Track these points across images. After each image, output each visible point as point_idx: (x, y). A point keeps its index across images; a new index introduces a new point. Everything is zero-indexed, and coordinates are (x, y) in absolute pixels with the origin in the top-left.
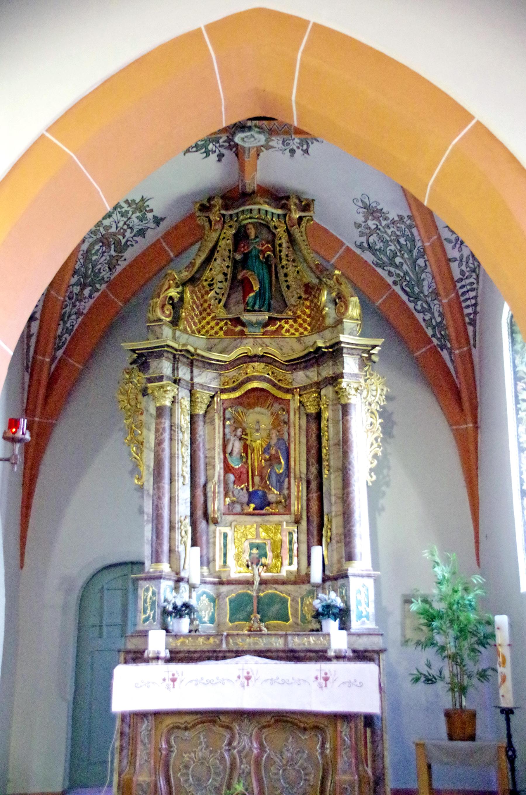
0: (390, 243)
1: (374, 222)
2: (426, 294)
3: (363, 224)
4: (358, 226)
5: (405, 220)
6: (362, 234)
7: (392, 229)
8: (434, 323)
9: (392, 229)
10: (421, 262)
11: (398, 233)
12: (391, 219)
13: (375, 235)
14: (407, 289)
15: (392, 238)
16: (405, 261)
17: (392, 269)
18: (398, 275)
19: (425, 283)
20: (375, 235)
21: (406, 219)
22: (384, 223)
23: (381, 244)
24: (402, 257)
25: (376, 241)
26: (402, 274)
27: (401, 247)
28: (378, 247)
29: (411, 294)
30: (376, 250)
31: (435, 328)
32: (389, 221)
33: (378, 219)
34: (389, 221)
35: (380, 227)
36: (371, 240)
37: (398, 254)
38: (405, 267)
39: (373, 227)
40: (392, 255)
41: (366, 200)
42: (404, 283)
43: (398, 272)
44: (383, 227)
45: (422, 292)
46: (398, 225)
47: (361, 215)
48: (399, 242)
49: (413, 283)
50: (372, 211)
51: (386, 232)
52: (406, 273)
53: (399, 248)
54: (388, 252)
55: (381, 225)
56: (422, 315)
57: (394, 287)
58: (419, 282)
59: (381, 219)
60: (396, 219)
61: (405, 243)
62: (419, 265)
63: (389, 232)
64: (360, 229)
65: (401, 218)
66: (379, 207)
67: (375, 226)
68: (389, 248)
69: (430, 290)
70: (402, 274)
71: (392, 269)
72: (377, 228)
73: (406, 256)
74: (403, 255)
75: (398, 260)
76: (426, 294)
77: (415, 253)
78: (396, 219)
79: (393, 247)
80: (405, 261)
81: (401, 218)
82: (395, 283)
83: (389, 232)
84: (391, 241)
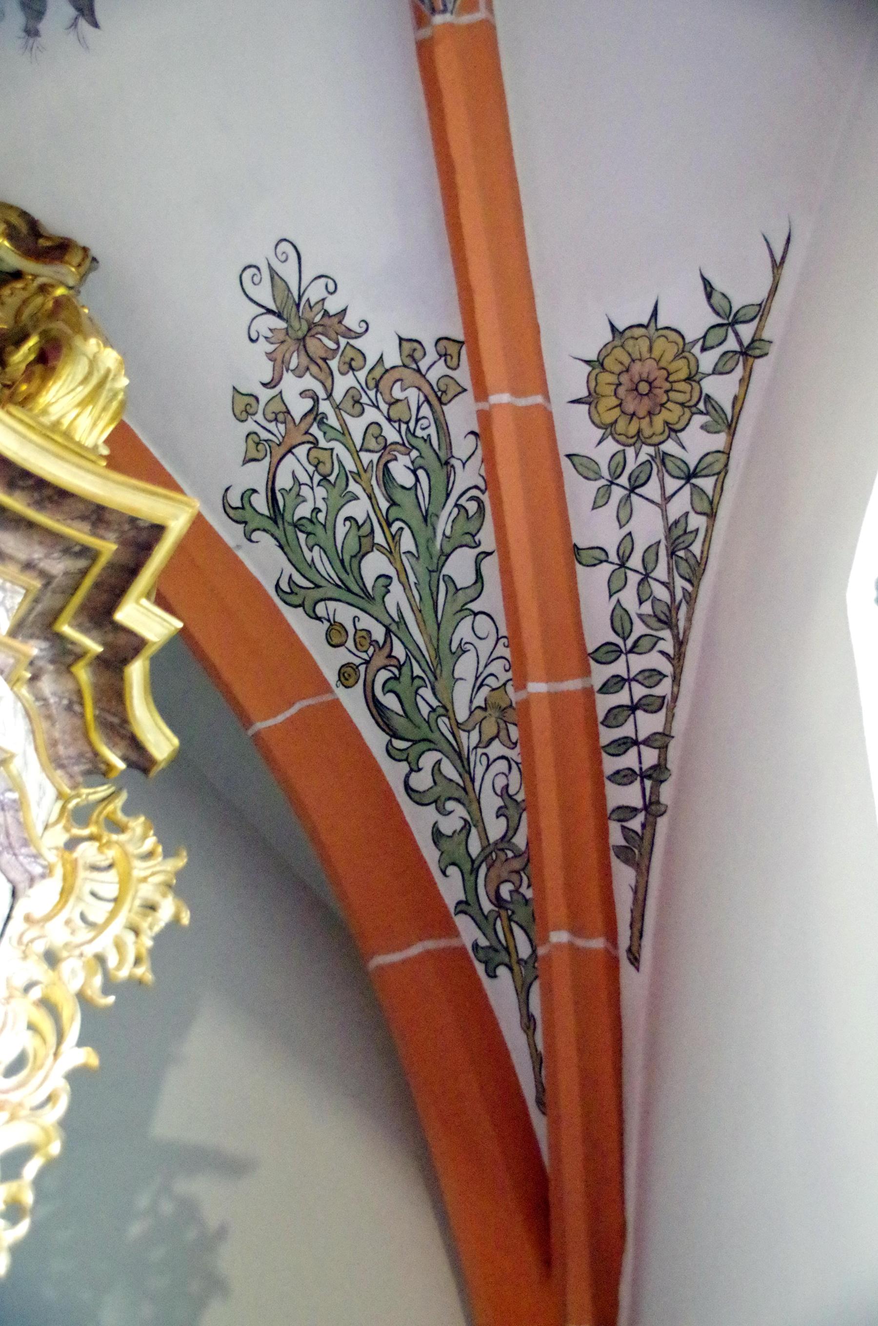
0: (353, 487)
1: (309, 382)
2: (462, 714)
3: (265, 395)
4: (244, 405)
5: (423, 365)
6: (256, 448)
7: (371, 415)
8: (475, 847)
9: (371, 415)
10: (460, 567)
11: (391, 434)
12: (371, 361)
13: (301, 451)
14: (390, 701)
15: (366, 457)
16: (402, 572)
17: (344, 614)
18: (364, 638)
19: (466, 667)
20: (301, 451)
21: (432, 354)
22: (343, 383)
23: (321, 492)
24: (390, 553)
25: (304, 478)
26: (379, 633)
27: (393, 503)
28: (304, 511)
29: (400, 723)
30: (297, 526)
31: (475, 871)
32: (362, 375)
33: (319, 364)
34: (362, 375)
35: (325, 407)
36: (283, 481)
37: (379, 538)
38: (396, 597)
39: (299, 407)
40: (352, 545)
41: (288, 272)
42: (384, 675)
43: (366, 622)
44: (337, 408)
45: (447, 710)
46: (397, 393)
47: (264, 346)
48: (387, 476)
49: (417, 671)
50: (306, 328)
51: (345, 431)
52: (394, 627)
53: (384, 504)
54: (341, 530)
55: (330, 396)
56: (430, 814)
57: (341, 693)
58: (440, 663)
59: (334, 364)
60: (393, 358)
61: (407, 480)
62: (449, 579)
63: (356, 427)
64: (250, 425)
65: (410, 347)
66: (333, 305)
67: (308, 404)
68: (350, 510)
69: (479, 701)
70: (379, 633)
71: (344, 614)
72: (315, 415)
73: (407, 542)
74: (395, 538)
75: (374, 565)
76: (462, 714)
77: (443, 525)
78: (393, 358)
79: (359, 509)
80: (402, 572)
81: (410, 347)
82: (346, 674)
83: (356, 427)
84: (357, 476)
